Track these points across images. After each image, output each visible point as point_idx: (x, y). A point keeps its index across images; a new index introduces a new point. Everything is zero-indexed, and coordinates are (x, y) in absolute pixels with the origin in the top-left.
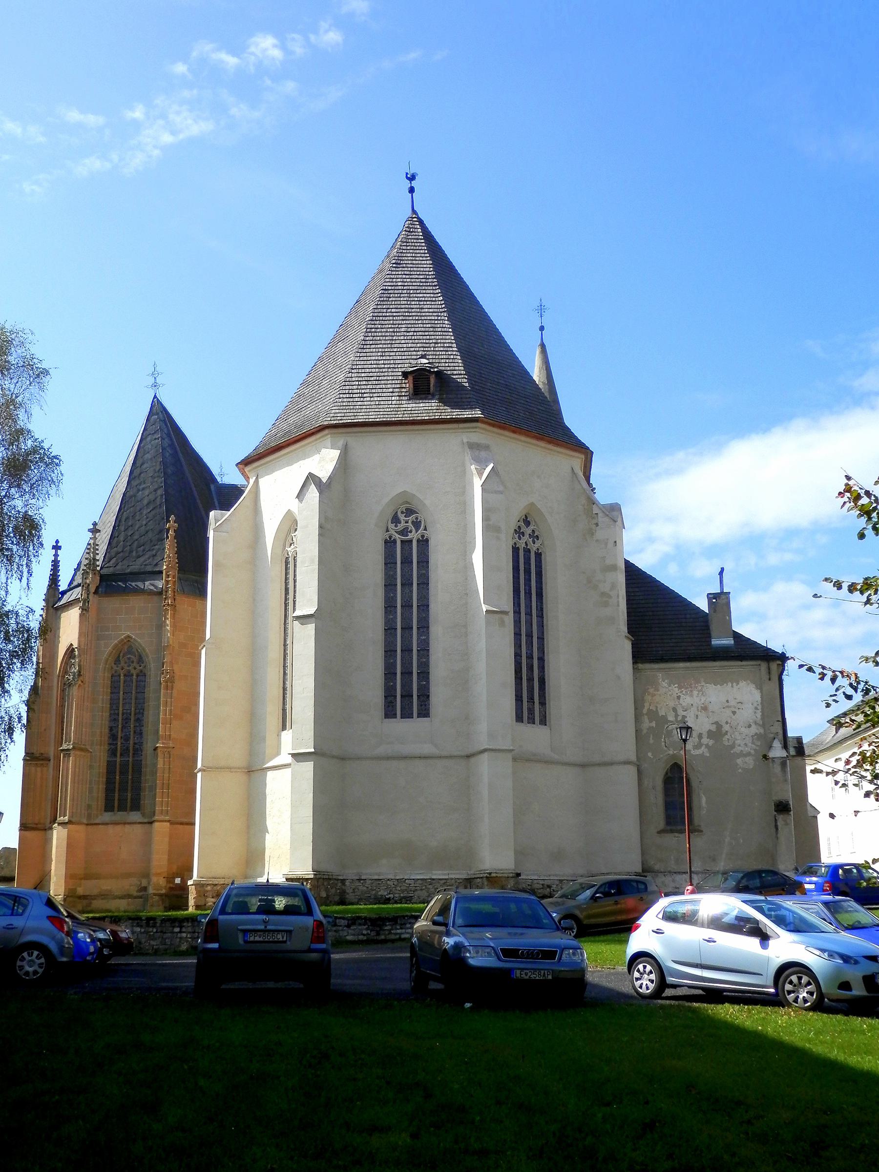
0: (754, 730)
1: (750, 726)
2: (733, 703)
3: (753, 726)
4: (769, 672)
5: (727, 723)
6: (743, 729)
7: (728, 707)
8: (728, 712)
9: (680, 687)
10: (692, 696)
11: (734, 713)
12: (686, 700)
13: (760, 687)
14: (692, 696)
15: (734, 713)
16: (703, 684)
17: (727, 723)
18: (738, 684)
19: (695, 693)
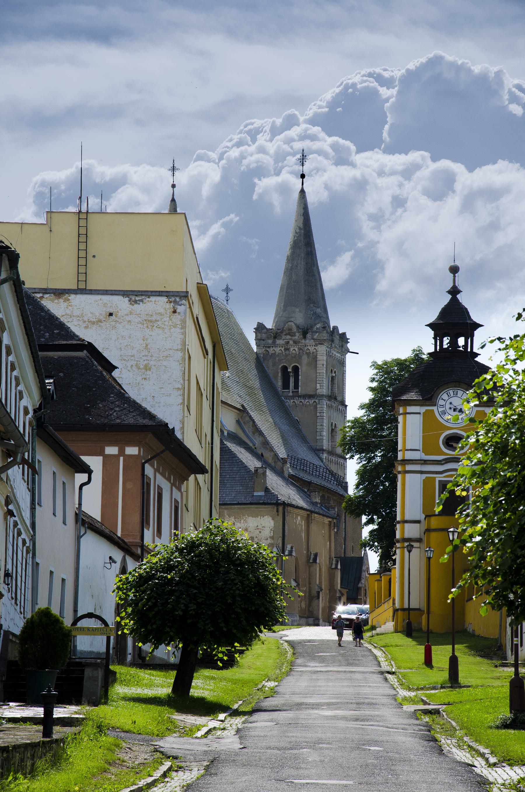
0: (269, 541)
1: (267, 539)
2: (260, 527)
3: (269, 539)
4: (277, 511)
5: (256, 537)
6: (264, 541)
7: (258, 529)
8: (258, 531)
9: (235, 518)
10: (240, 523)
11: (260, 532)
12: (238, 525)
13: (273, 519)
14: (240, 523)
15: (260, 532)
16: (247, 516)
17: (256, 537)
18: (263, 517)
19: (242, 521)
